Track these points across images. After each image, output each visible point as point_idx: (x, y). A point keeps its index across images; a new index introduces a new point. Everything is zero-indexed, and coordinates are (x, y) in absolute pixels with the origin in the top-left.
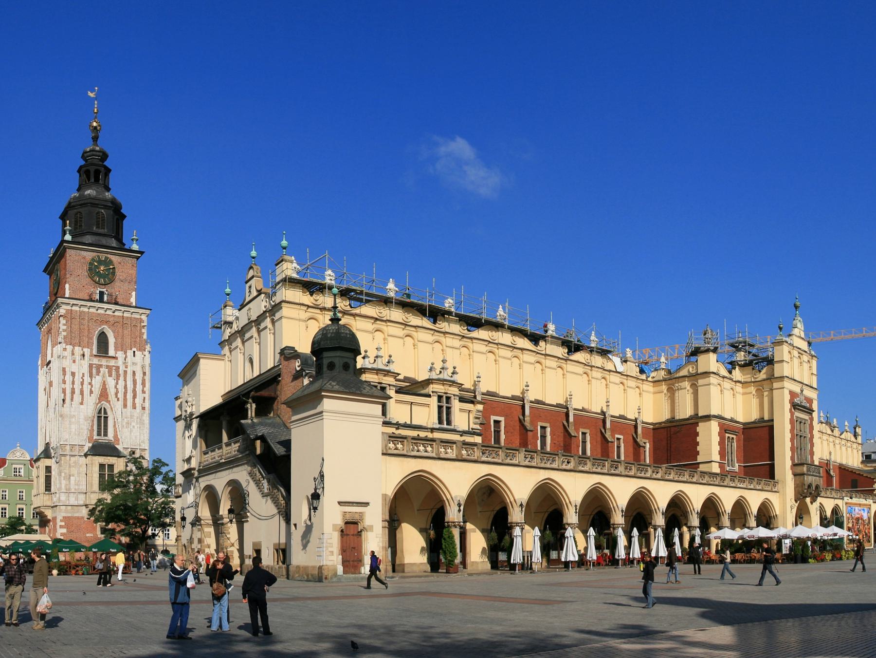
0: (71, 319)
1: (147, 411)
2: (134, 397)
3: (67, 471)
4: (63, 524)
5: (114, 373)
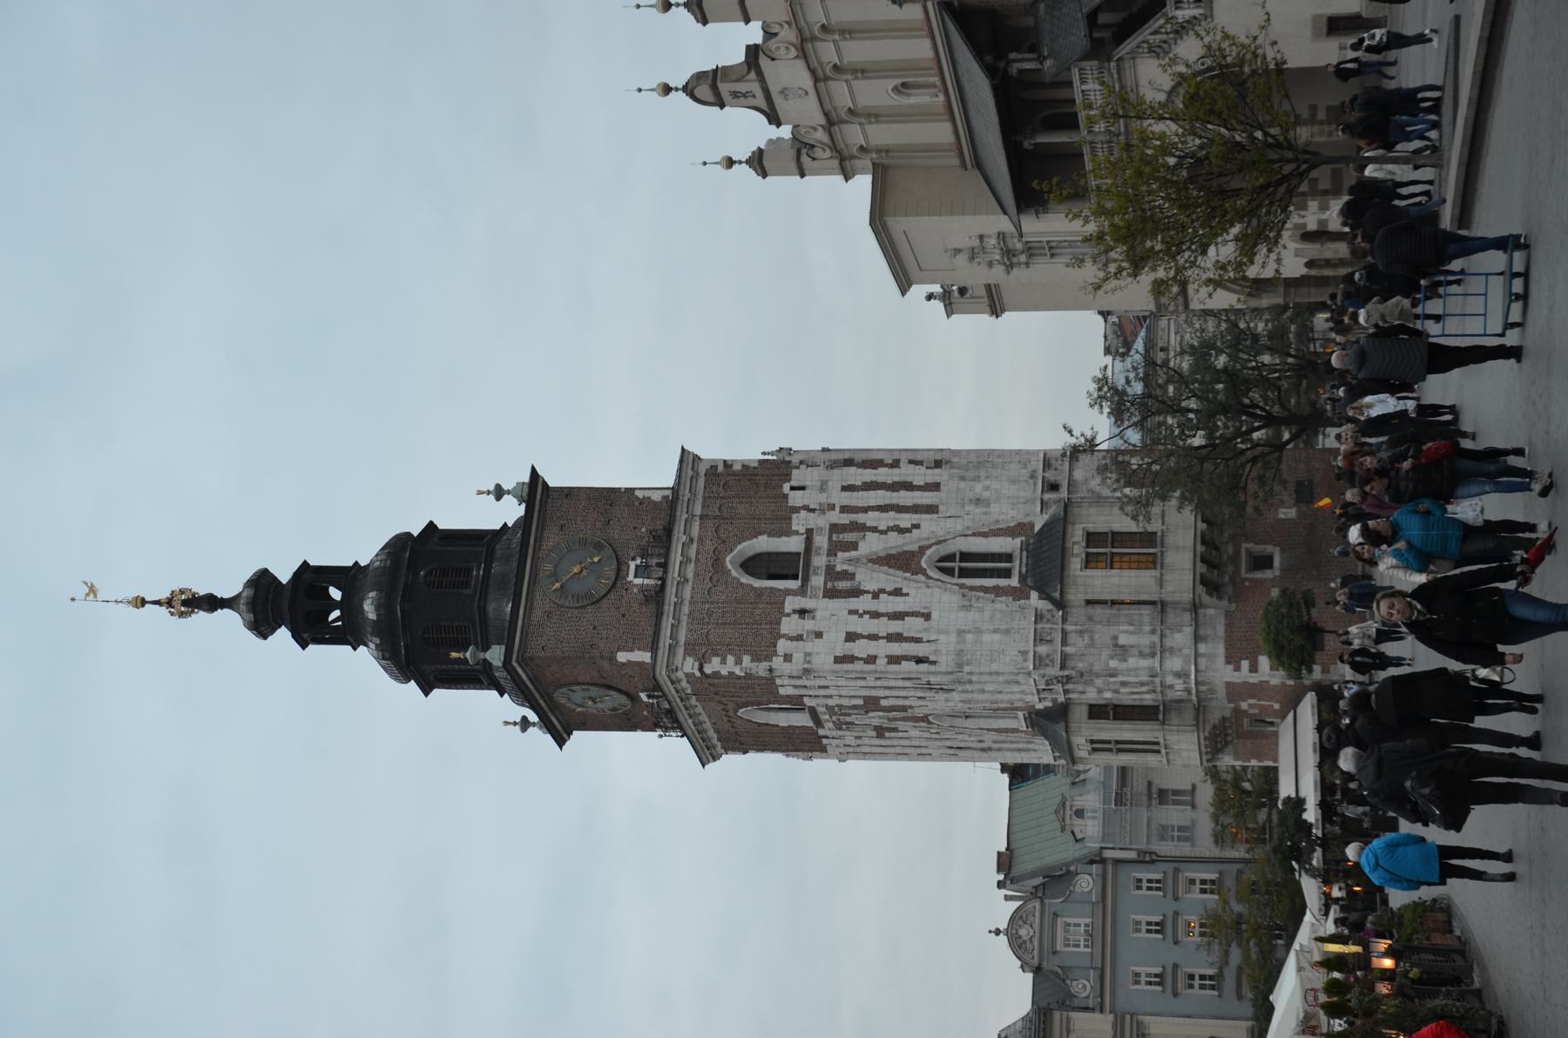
2: (908, 486)
4: (1245, 664)
5: (849, 537)
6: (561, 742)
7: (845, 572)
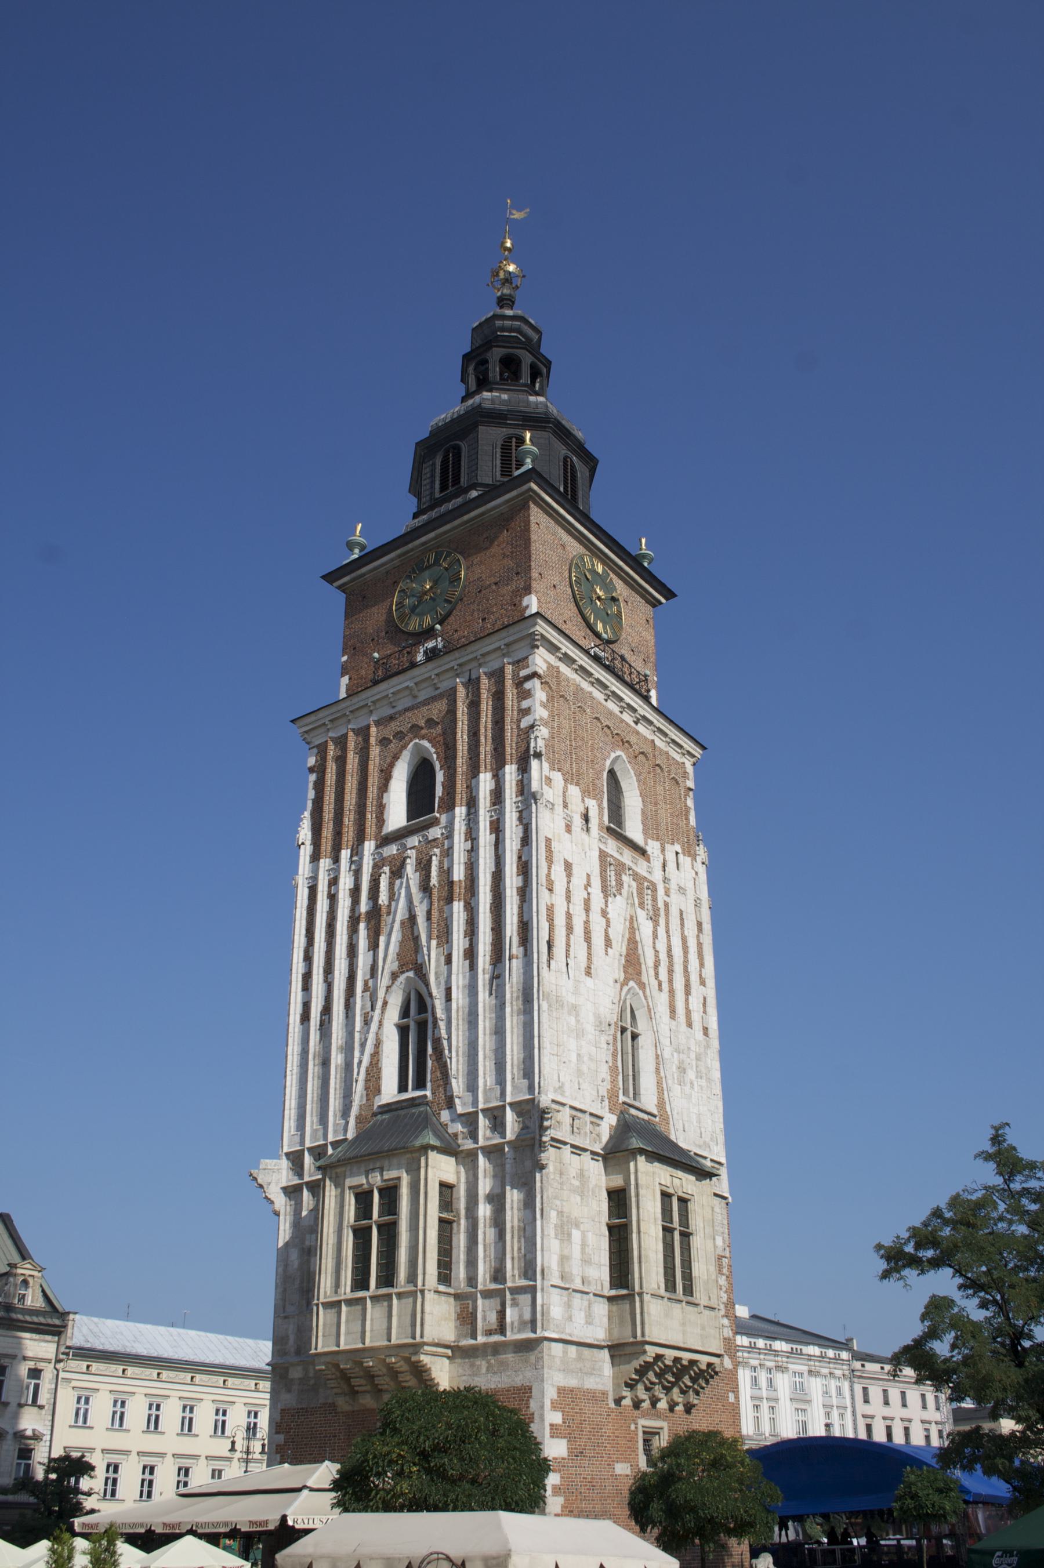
1: (715, 1044)
6: (330, 577)
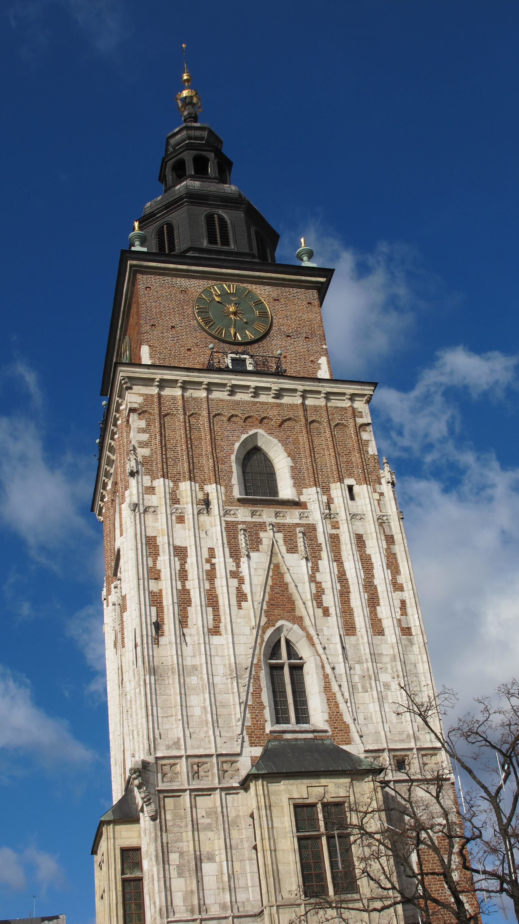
0: (162, 416)
2: (373, 601)
3: (188, 846)
7: (259, 541)
